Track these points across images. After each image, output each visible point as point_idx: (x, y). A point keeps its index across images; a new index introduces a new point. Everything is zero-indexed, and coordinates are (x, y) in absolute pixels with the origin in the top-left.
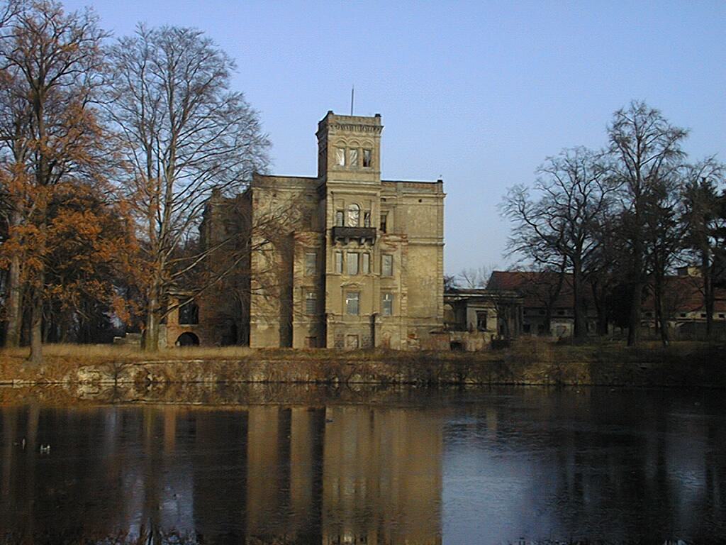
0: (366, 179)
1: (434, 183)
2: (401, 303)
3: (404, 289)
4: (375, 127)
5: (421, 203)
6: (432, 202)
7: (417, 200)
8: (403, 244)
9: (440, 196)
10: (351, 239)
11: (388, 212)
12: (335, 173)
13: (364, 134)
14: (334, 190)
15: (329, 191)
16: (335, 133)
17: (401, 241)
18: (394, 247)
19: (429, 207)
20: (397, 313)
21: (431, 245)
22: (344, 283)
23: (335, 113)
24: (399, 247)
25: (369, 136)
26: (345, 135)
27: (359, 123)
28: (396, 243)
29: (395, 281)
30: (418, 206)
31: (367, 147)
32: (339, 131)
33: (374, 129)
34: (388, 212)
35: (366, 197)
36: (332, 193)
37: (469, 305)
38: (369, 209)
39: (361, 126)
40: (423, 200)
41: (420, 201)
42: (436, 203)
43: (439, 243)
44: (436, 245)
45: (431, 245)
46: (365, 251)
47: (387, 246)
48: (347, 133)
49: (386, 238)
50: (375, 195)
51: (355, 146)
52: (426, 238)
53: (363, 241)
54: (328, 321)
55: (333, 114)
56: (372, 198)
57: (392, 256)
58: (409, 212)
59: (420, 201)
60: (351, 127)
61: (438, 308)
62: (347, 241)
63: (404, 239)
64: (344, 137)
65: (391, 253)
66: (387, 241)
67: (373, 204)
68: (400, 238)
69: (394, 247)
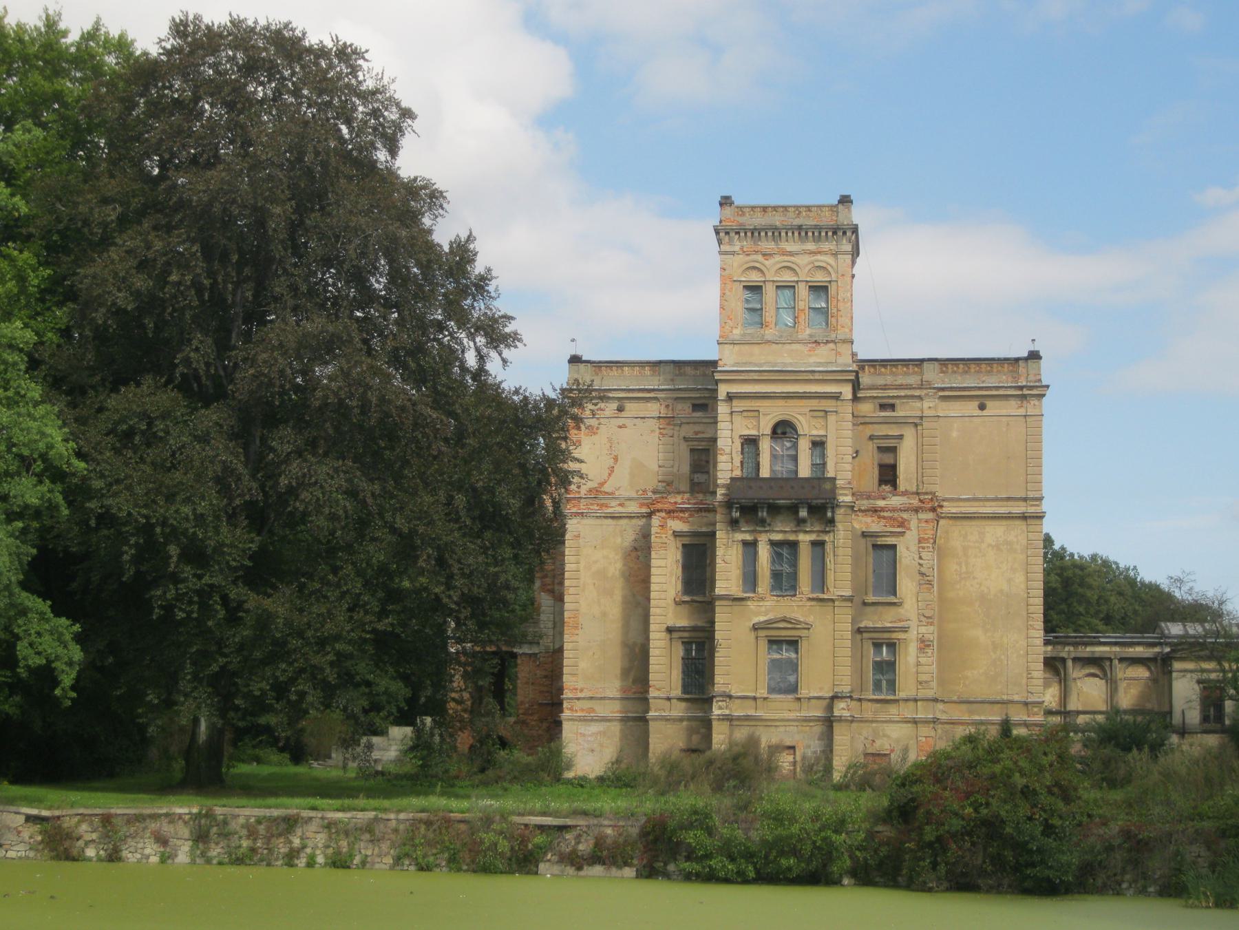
0: (820, 358)
1: (1017, 360)
2: (918, 664)
3: (923, 630)
4: (836, 230)
5: (985, 413)
6: (1012, 407)
7: (976, 403)
8: (922, 516)
9: (1032, 392)
10: (774, 509)
11: (901, 437)
12: (737, 347)
13: (810, 246)
14: (735, 389)
15: (723, 390)
16: (737, 248)
17: (916, 510)
18: (902, 524)
19: (1004, 419)
20: (906, 688)
21: (1009, 517)
22: (756, 620)
23: (738, 201)
24: (913, 524)
25: (825, 253)
26: (764, 255)
27: (797, 222)
28: (905, 516)
29: (901, 610)
30: (979, 420)
31: (820, 278)
32: (747, 244)
33: (835, 233)
34: (901, 437)
35: (814, 403)
36: (730, 397)
37: (1177, 665)
38: (822, 433)
39: (800, 228)
40: (989, 404)
41: (982, 407)
42: (1022, 412)
43: (1031, 510)
44: (1024, 517)
45: (1009, 517)
46: (813, 537)
47: (883, 522)
48: (767, 245)
49: (881, 503)
50: (836, 397)
51: (788, 277)
52: (996, 499)
53: (803, 513)
54: (716, 711)
55: (731, 203)
56: (829, 405)
57: (894, 547)
58: (955, 434)
59: (982, 407)
60: (775, 232)
61: (1029, 672)
62: (763, 514)
63: (932, 506)
64: (760, 258)
65: (890, 541)
66: (883, 509)
67: (832, 418)
68: (915, 502)
69: (902, 525)
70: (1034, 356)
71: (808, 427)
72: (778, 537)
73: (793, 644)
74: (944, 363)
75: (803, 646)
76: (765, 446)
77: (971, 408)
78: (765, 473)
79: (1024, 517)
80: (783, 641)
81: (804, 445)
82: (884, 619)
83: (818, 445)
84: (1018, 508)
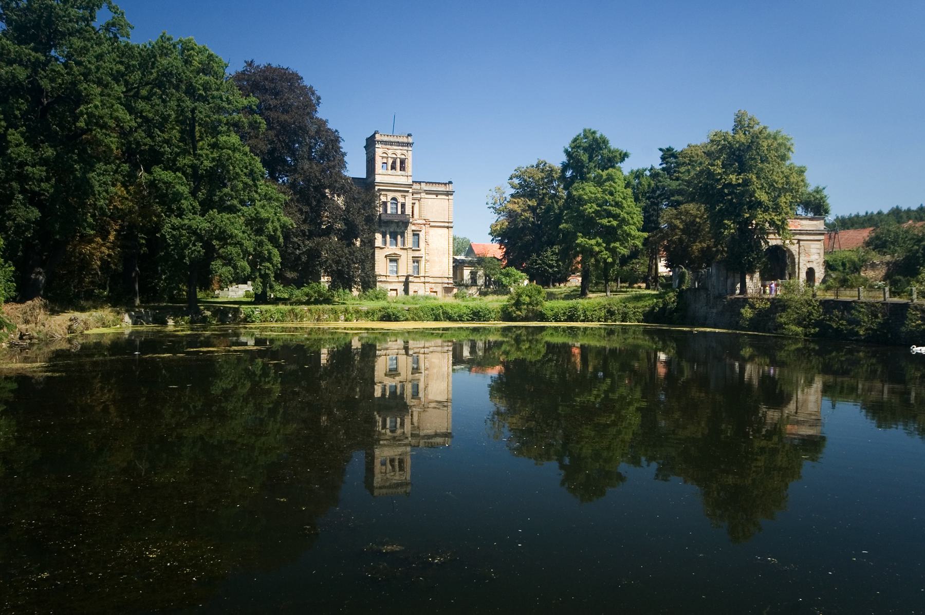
15: (377, 188)
50: (408, 192)
70: (450, 183)
71: (401, 200)
72: (392, 230)
73: (396, 261)
74: (426, 183)
75: (400, 261)
76: (389, 204)
77: (434, 196)
78: (389, 212)
79: (448, 227)
80: (394, 259)
81: (399, 205)
82: (417, 254)
83: (403, 205)
84: (447, 225)
